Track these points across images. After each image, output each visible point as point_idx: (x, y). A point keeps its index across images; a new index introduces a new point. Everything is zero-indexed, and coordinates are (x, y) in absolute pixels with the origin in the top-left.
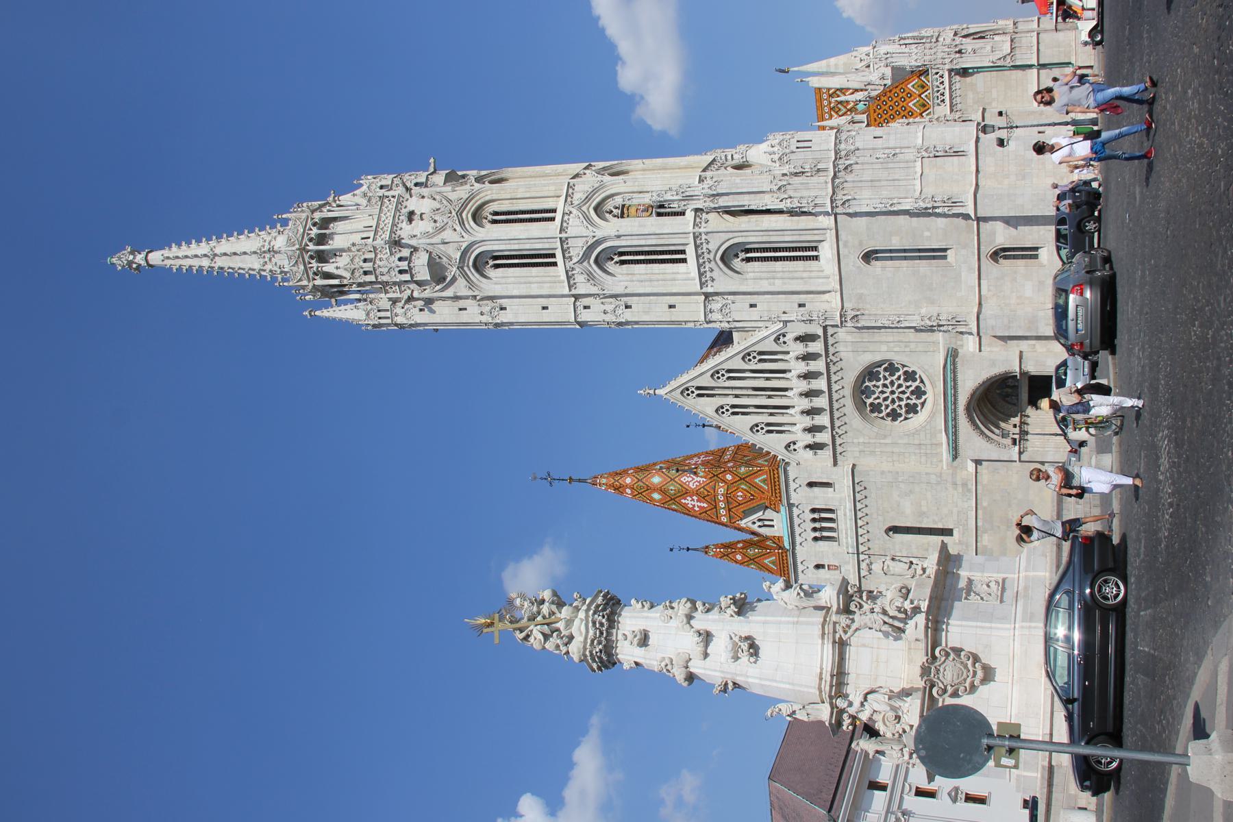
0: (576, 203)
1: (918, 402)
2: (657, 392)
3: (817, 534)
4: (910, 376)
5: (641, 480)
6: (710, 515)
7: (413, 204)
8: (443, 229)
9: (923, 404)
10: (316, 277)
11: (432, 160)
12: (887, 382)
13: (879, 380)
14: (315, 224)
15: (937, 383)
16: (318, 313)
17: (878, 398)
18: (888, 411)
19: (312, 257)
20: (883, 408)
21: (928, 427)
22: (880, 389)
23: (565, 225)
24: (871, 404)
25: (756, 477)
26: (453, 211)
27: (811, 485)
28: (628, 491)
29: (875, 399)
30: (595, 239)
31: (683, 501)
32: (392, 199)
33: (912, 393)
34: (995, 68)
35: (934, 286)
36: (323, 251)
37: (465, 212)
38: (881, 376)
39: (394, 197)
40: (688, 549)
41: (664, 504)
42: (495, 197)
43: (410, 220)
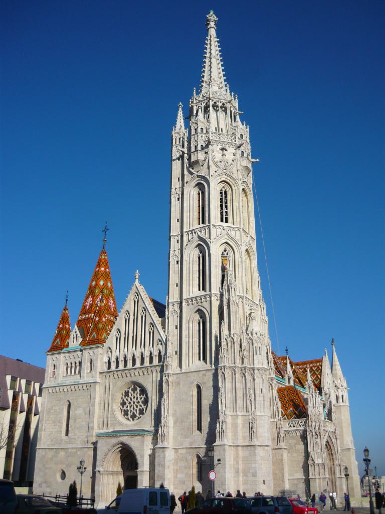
0: (229, 232)
1: (129, 416)
2: (137, 280)
3: (69, 365)
4: (141, 412)
5: (102, 275)
6: (84, 311)
7: (231, 150)
8: (217, 166)
9: (128, 419)
11: (258, 160)
13: (140, 395)
15: (136, 426)
16: (180, 109)
18: (125, 400)
20: (127, 398)
21: (116, 422)
22: (135, 396)
24: (128, 391)
25: (96, 333)
27: (91, 360)
28: (97, 269)
30: (209, 243)
31: (90, 297)
33: (134, 413)
34: (307, 455)
35: (183, 424)
37: (225, 177)
38: (142, 396)
39: (235, 141)
40: (67, 300)
41: (91, 287)
42: (234, 191)
43: (222, 149)
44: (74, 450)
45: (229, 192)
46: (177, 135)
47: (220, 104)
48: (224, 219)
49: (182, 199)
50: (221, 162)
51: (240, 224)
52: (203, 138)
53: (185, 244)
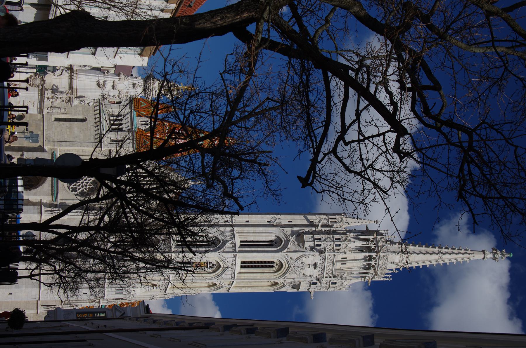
8: (297, 259)
10: (372, 240)
12: (85, 187)
13: (89, 188)
14: (373, 266)
15: (61, 186)
17: (89, 180)
19: (374, 249)
22: (88, 184)
23: (234, 259)
26: (293, 268)
29: (91, 180)
30: (219, 251)
32: (327, 276)
36: (369, 252)
42: (272, 274)
44: (42, 129)
45: (272, 270)
46: (340, 220)
47: (373, 263)
48: (245, 265)
49: (269, 225)
50: (302, 263)
51: (238, 279)
52: (329, 247)
53: (222, 229)
